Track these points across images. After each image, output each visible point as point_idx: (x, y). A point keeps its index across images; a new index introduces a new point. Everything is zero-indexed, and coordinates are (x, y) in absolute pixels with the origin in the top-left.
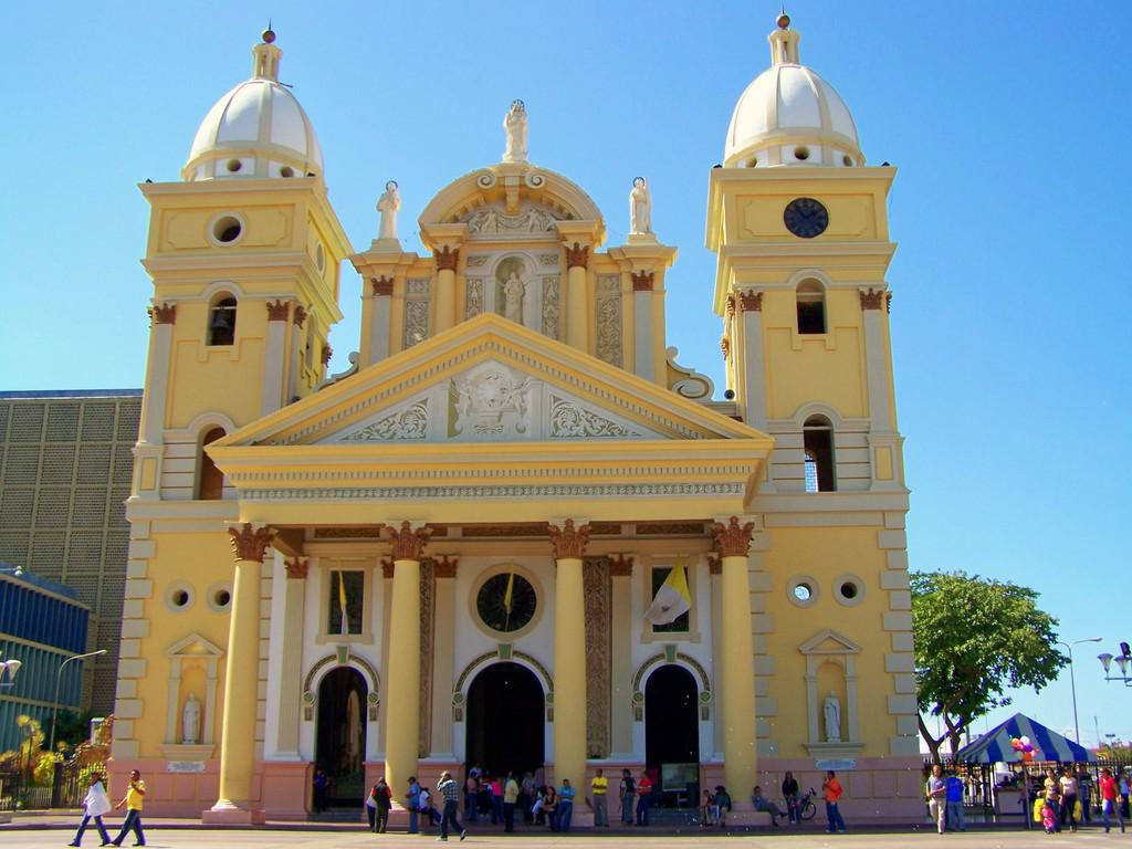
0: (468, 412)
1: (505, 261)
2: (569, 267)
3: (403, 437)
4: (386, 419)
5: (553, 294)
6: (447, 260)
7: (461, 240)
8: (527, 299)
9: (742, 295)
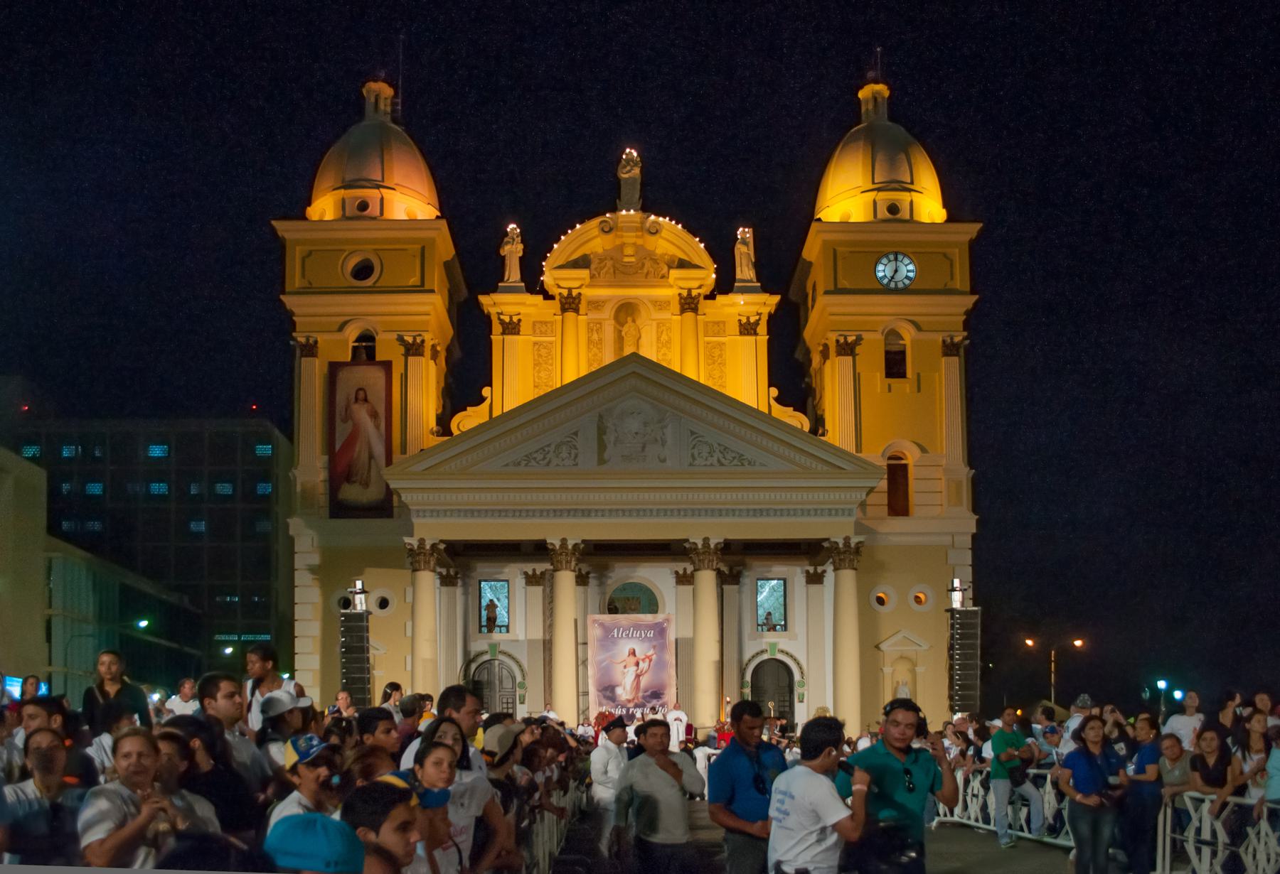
0: (615, 444)
1: (623, 304)
3: (557, 465)
4: (542, 449)
9: (838, 341)
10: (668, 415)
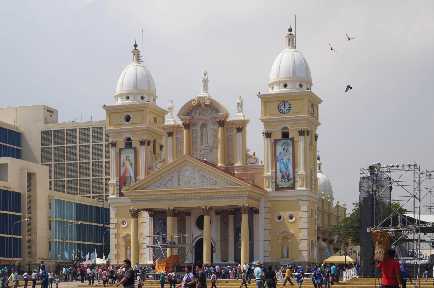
0: (182, 179)
1: (203, 124)
2: (219, 127)
4: (163, 182)
5: (216, 134)
6: (187, 126)
7: (190, 120)
8: (209, 136)
10: (196, 170)
